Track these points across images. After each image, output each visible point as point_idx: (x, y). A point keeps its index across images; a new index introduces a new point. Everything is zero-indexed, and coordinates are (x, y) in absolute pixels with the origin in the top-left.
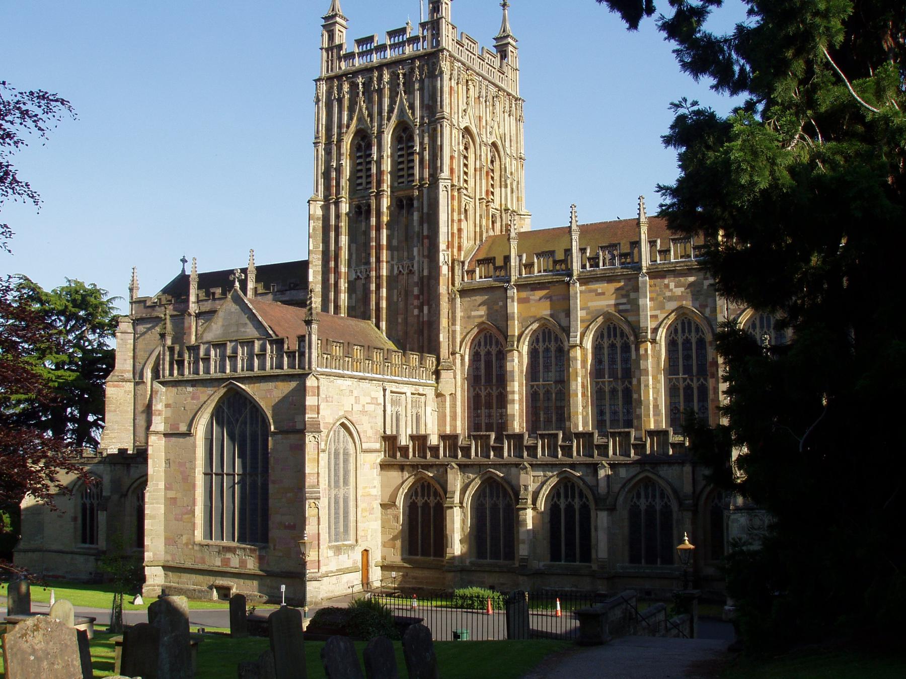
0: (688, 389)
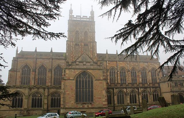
0: (134, 79)
